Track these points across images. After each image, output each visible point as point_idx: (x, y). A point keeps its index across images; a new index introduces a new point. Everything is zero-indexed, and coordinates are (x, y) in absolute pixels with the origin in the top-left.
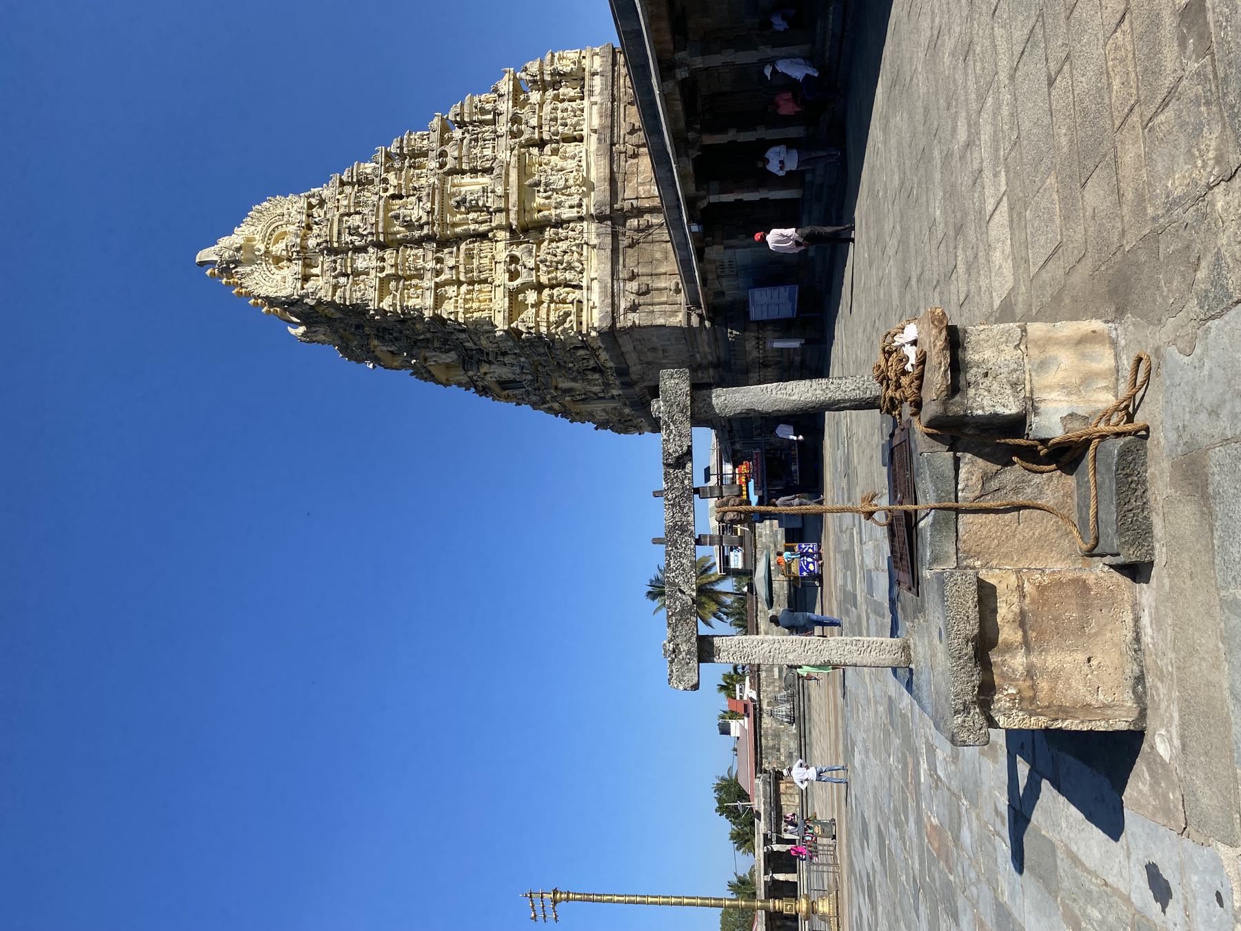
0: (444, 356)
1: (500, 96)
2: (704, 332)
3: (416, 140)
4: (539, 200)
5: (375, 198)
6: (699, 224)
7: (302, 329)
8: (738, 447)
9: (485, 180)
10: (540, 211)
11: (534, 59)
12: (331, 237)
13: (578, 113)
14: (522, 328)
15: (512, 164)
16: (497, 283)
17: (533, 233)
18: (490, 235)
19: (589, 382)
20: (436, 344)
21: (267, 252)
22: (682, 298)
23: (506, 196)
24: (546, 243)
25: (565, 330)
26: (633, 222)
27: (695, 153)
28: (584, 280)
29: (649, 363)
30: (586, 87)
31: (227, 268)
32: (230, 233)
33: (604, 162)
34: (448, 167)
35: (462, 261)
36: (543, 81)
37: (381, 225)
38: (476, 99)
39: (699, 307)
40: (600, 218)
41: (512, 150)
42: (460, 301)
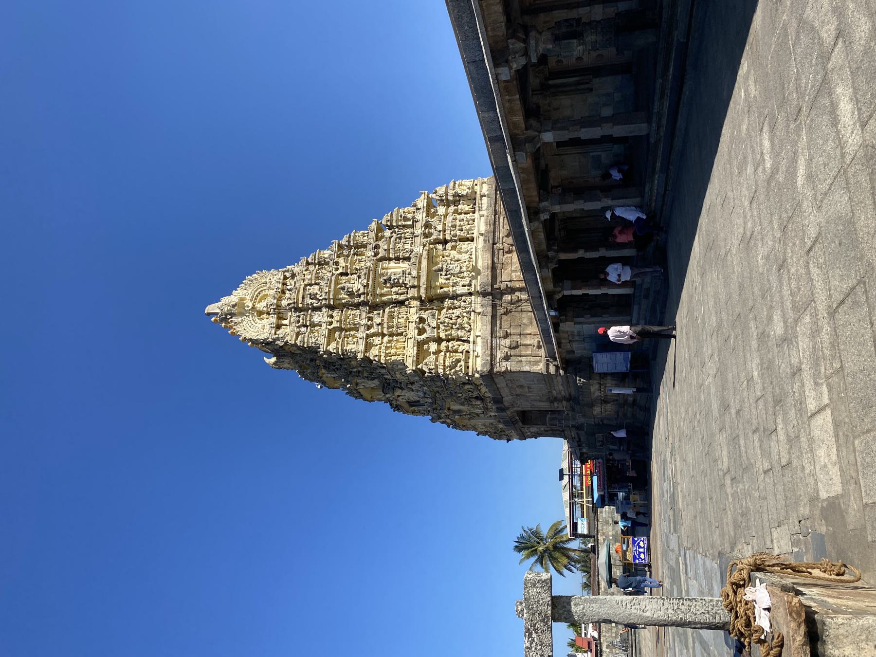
0: (370, 382)
1: (418, 209)
2: (559, 377)
3: (359, 236)
4: (441, 280)
5: (329, 274)
6: (555, 310)
7: (274, 359)
8: (584, 450)
9: (405, 265)
10: (441, 288)
11: (441, 185)
12: (298, 300)
14: (425, 369)
15: (424, 256)
16: (409, 336)
17: (436, 303)
18: (406, 303)
19: (473, 406)
20: (365, 374)
22: (542, 352)
23: (419, 277)
24: (445, 310)
25: (456, 372)
26: (508, 297)
28: (471, 337)
29: (517, 395)
30: (477, 205)
31: (225, 318)
32: (230, 294)
34: (380, 255)
35: (385, 320)
36: (447, 200)
37: (332, 293)
38: (401, 211)
39: (555, 360)
40: (484, 294)
41: (424, 246)
42: (383, 348)
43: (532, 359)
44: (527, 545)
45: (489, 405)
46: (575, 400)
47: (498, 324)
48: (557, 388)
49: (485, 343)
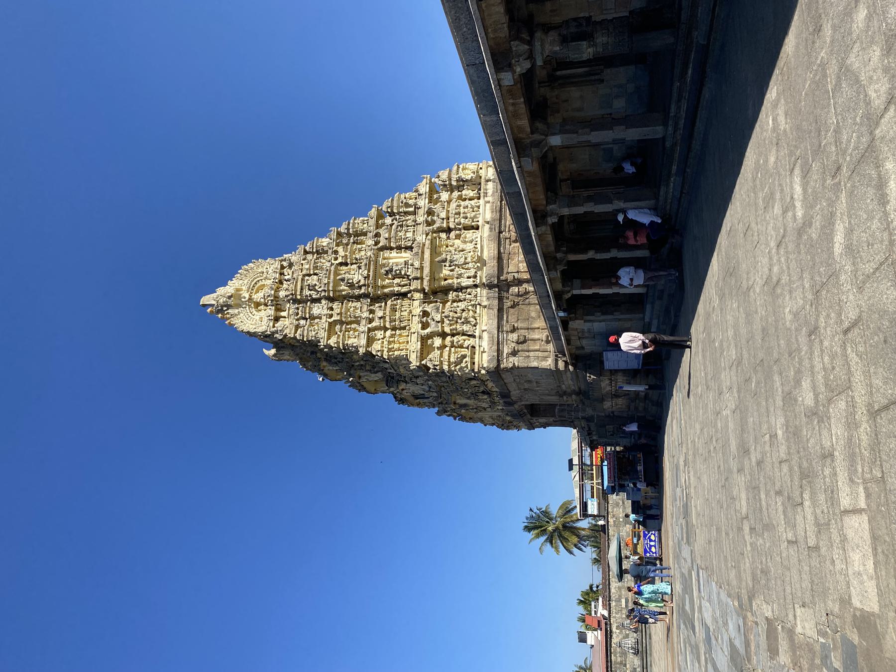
0: (373, 375)
1: (420, 195)
3: (359, 223)
4: (446, 272)
5: (329, 264)
6: (564, 311)
7: (273, 351)
8: (595, 438)
9: (406, 255)
10: (445, 280)
11: (444, 169)
12: (296, 291)
13: (476, 209)
15: (427, 246)
16: (413, 330)
17: (440, 295)
18: (409, 295)
19: (479, 400)
20: (368, 368)
22: (551, 347)
23: (421, 268)
24: (449, 303)
25: (461, 368)
26: (514, 290)
27: (561, 268)
28: (477, 331)
29: (525, 389)
30: (482, 190)
31: (222, 309)
32: (225, 284)
33: (494, 246)
34: (381, 244)
35: (388, 313)
36: (451, 184)
37: (331, 285)
38: (402, 196)
39: (564, 355)
40: (490, 286)
41: (427, 235)
42: (386, 343)
43: (540, 354)
44: (537, 524)
45: (497, 399)
46: (584, 393)
47: (505, 318)
48: (566, 383)
49: (491, 338)
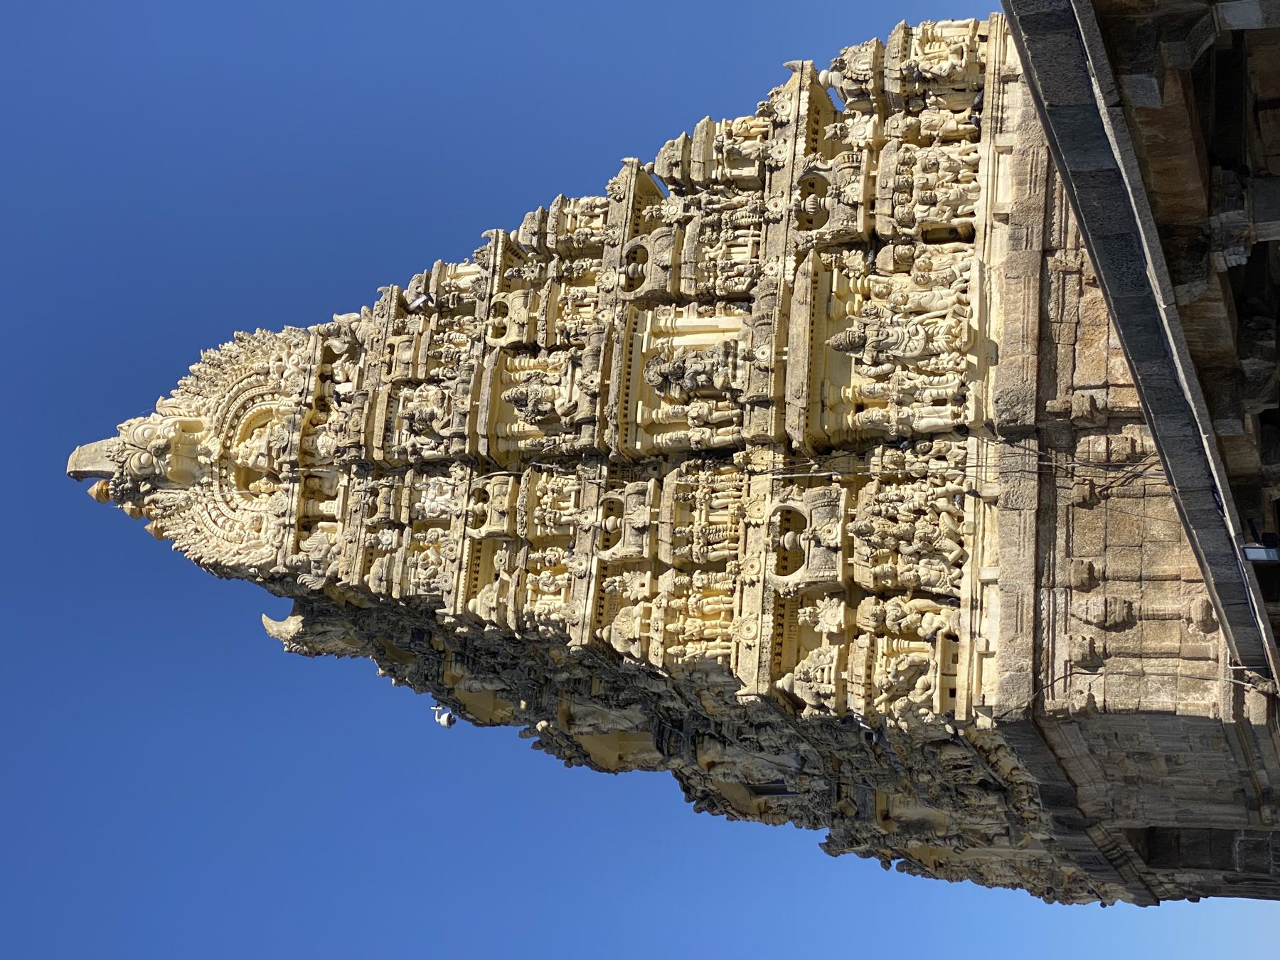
0: (614, 713)
1: (782, 125)
3: (578, 216)
4: (861, 381)
7: (293, 625)
9: (728, 325)
10: (860, 408)
11: (860, 40)
12: (369, 434)
13: (964, 172)
15: (799, 294)
16: (748, 575)
18: (738, 457)
20: (598, 689)
21: (225, 457)
22: (1218, 643)
23: (780, 369)
24: (871, 487)
25: (910, 708)
26: (1094, 445)
27: (1256, 406)
29: (1128, 780)
30: (987, 111)
33: (1026, 297)
34: (646, 286)
35: (665, 515)
36: (881, 91)
37: (483, 417)
38: (721, 128)
40: (1012, 433)
41: (801, 257)
42: (657, 614)
43: (1181, 666)
45: (1029, 809)
47: (1061, 542)
49: (1012, 605)
